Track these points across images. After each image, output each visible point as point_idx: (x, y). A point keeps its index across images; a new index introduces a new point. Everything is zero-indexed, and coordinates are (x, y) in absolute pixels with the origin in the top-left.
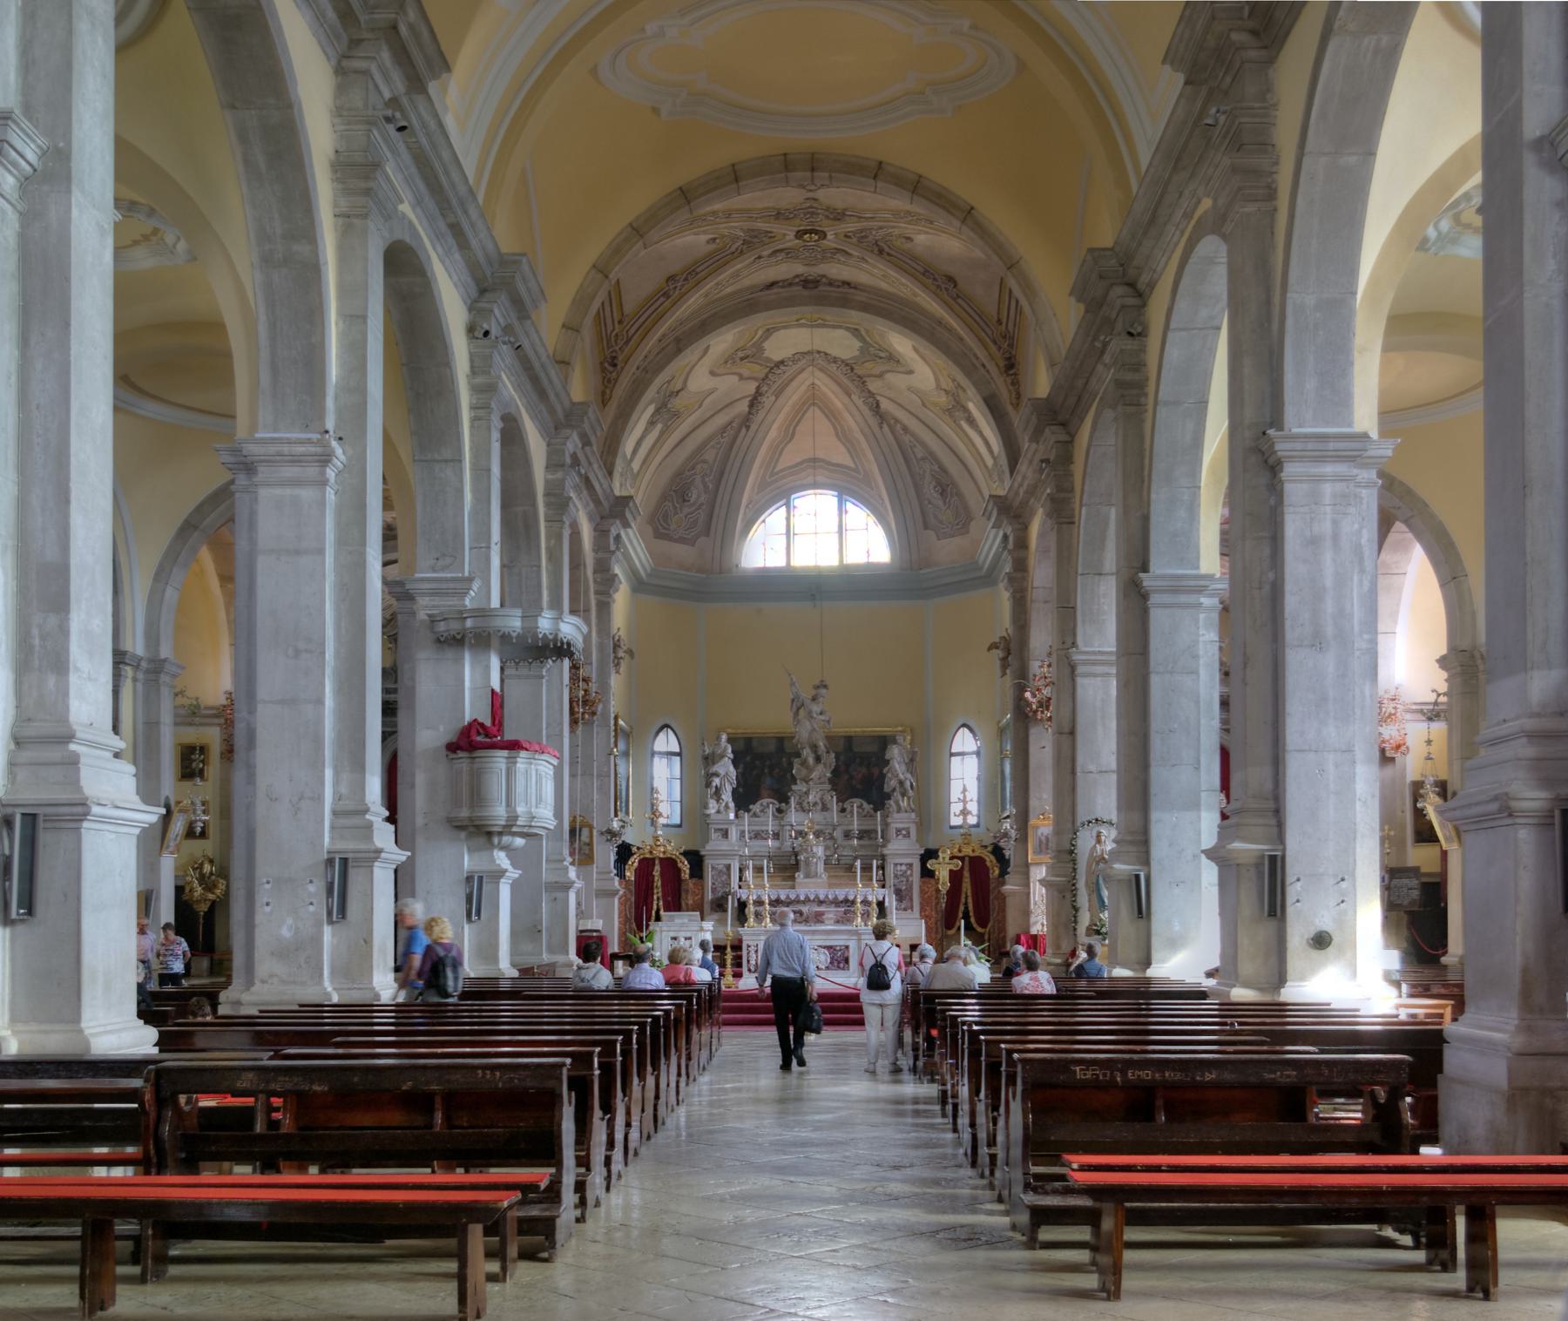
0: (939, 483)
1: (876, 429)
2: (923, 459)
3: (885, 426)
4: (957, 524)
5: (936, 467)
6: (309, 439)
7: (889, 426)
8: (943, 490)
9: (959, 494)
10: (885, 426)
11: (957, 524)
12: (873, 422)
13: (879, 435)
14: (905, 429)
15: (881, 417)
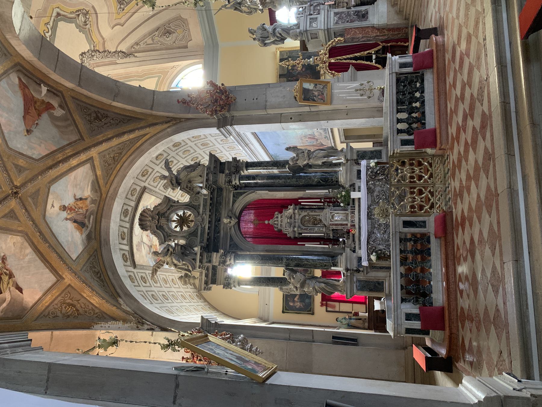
0: (164, 34)
1: (137, 59)
2: (153, 40)
3: (136, 54)
4: (183, 26)
5: (157, 33)
6: (125, 213)
7: (136, 52)
8: (168, 32)
9: (169, 22)
10: (136, 54)
11: (183, 26)
12: (132, 59)
13: (141, 59)
14: (137, 44)
15: (131, 54)
